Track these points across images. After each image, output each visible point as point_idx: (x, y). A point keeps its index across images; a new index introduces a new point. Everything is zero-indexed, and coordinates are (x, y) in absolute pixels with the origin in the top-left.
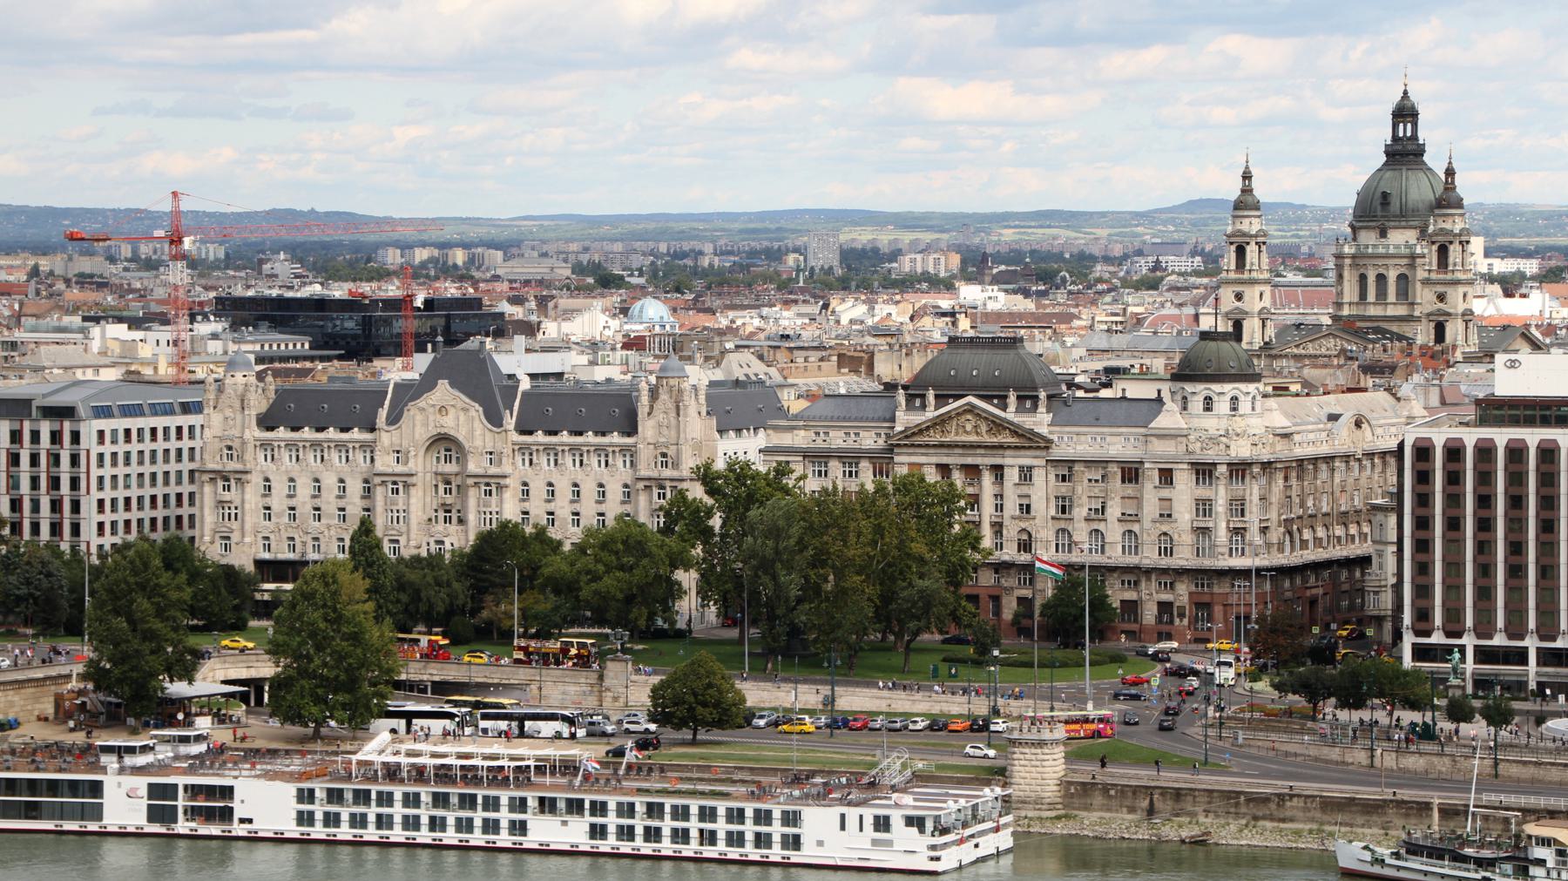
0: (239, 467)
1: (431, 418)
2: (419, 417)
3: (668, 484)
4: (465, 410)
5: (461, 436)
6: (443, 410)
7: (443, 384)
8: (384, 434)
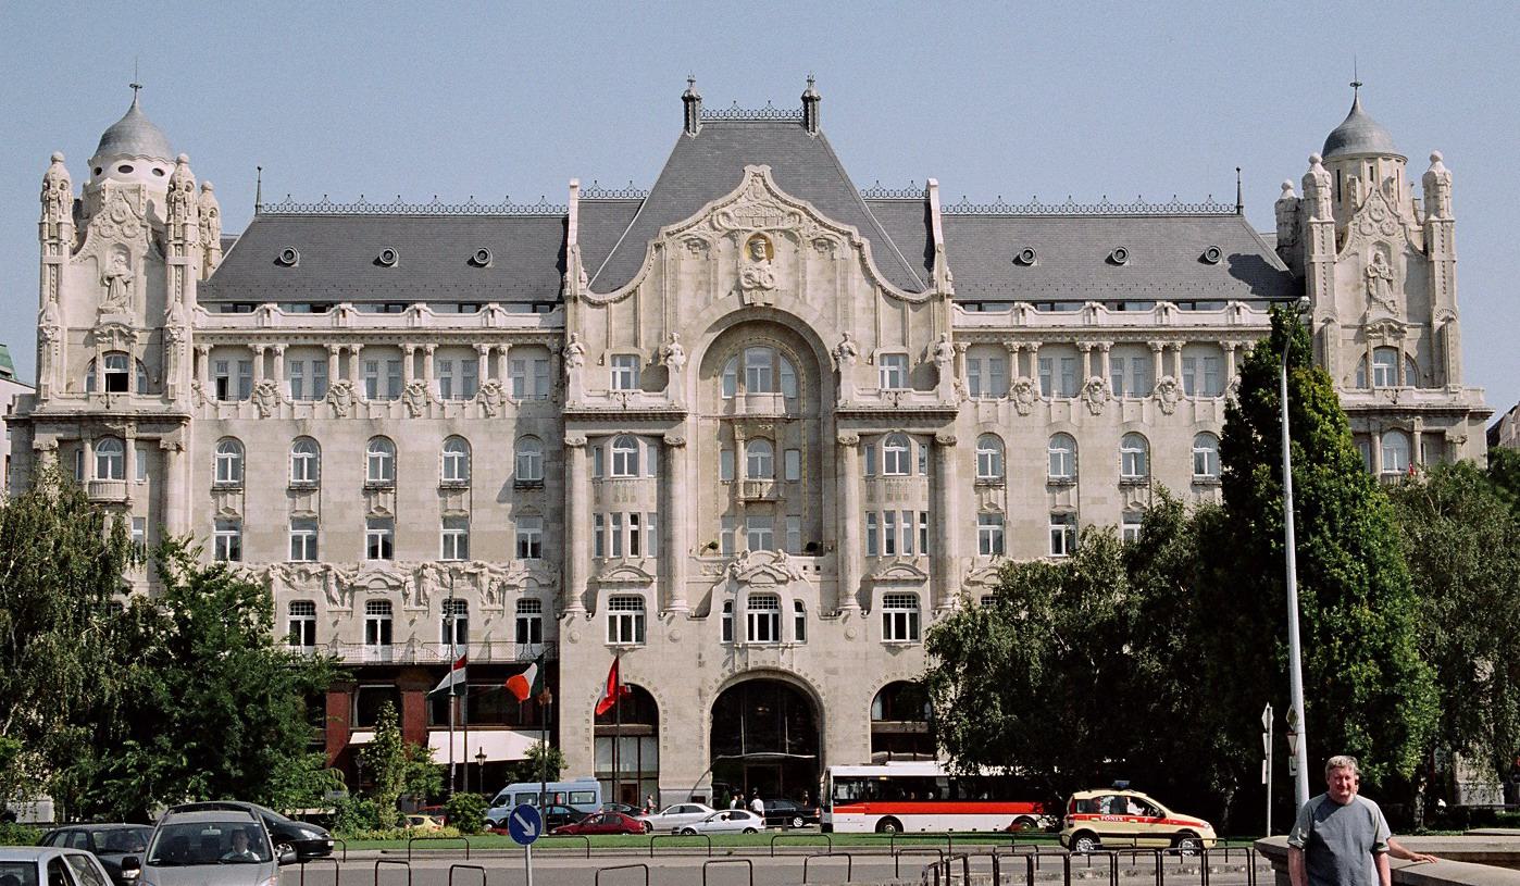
0: (153, 405)
1: (724, 266)
5: (812, 312)
6: (758, 245)
7: (756, 179)
8: (584, 308)
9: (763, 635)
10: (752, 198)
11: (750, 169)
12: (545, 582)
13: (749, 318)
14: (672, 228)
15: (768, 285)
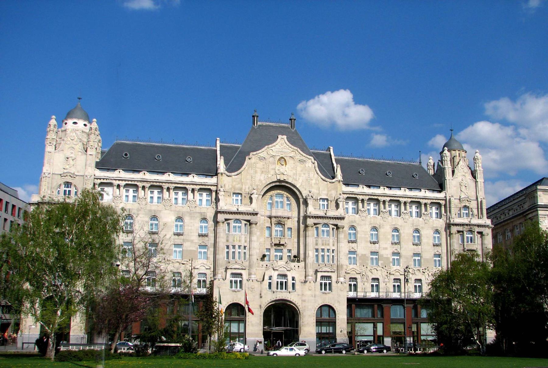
2: (260, 164)
3: (477, 229)
7: (282, 139)
9: (282, 288)
10: (282, 145)
11: (280, 136)
12: (208, 267)
13: (278, 184)
14: (254, 153)
15: (285, 173)
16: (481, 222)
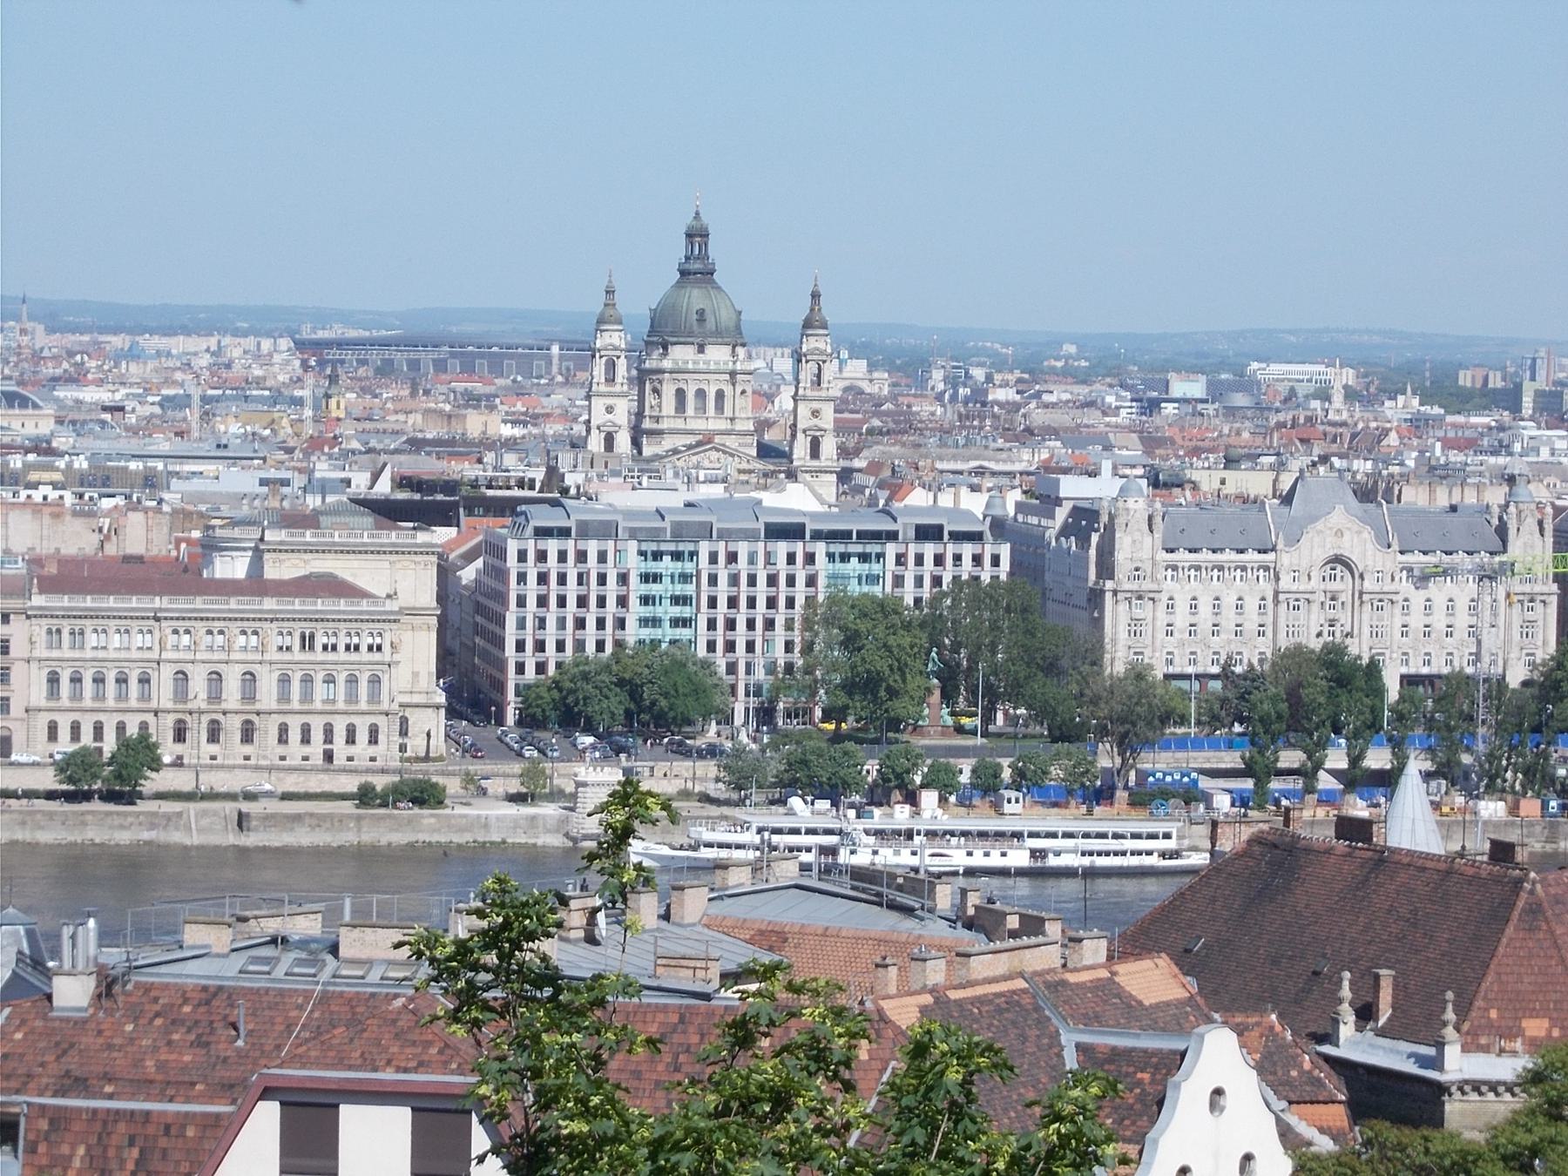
3: (1540, 598)
4: (1359, 533)
5: (1354, 556)
6: (1340, 533)
16: (1545, 589)
